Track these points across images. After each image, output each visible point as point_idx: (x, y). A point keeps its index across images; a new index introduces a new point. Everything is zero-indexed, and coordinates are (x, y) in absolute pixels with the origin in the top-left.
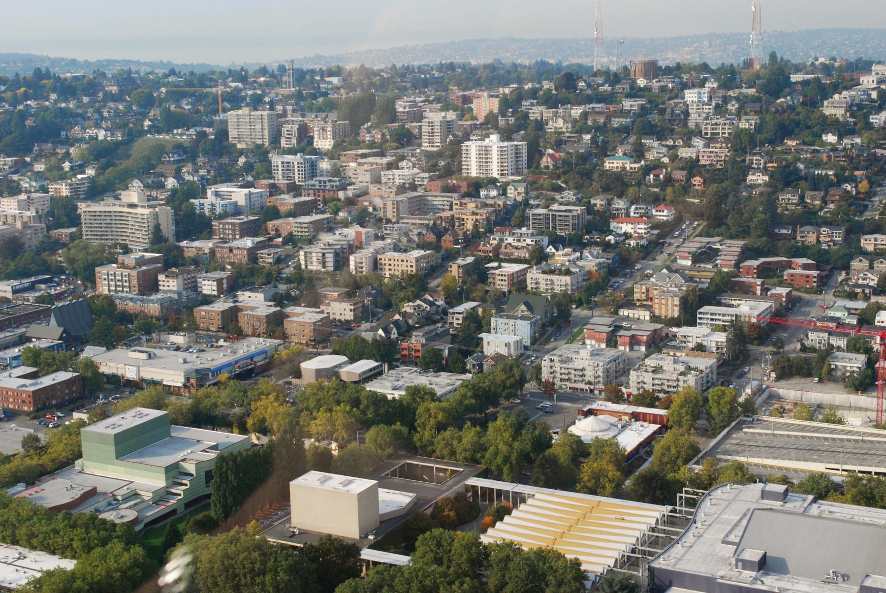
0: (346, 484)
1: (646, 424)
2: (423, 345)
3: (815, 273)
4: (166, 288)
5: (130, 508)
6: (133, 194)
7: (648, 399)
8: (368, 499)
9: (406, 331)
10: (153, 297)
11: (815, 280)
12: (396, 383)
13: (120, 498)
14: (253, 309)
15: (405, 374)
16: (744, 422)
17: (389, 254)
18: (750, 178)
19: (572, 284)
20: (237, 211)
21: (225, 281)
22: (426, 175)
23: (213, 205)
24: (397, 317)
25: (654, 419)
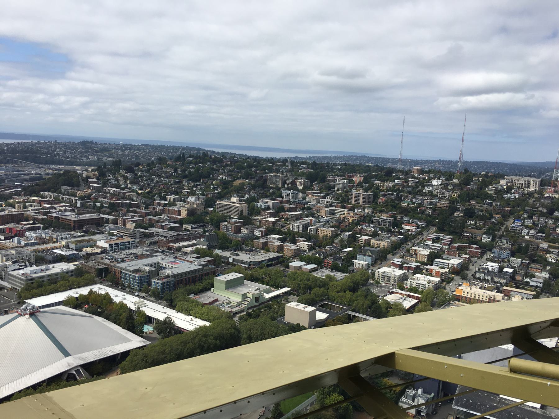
0: (304, 308)
1: (413, 299)
2: (332, 262)
3: (480, 251)
4: (244, 232)
5: (229, 307)
6: (234, 199)
7: (414, 290)
8: (313, 314)
9: (326, 256)
10: (239, 235)
11: (479, 254)
12: (322, 274)
13: (225, 303)
14: (273, 242)
15: (325, 271)
16: (451, 303)
17: (322, 228)
18: (456, 213)
19: (387, 246)
20: (268, 208)
21: (264, 232)
22: (336, 202)
23: (261, 205)
24: (324, 251)
25: (417, 298)
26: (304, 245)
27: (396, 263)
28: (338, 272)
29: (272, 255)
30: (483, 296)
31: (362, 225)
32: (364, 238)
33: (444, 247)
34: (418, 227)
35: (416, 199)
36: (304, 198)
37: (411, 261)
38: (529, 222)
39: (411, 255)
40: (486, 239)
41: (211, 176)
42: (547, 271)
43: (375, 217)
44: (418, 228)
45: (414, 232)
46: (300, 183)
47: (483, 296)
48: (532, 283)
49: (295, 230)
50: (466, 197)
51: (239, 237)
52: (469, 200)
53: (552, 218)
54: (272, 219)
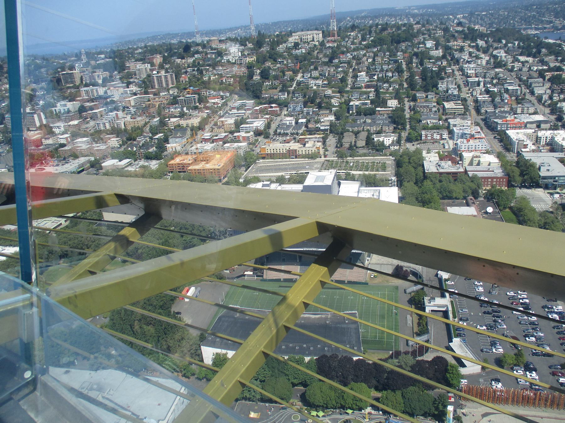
4: (46, 143)
10: (41, 147)
15: (140, 163)
22: (140, 89)
26: (114, 142)
27: (206, 138)
28: (152, 161)
29: (82, 160)
30: (283, 149)
31: (169, 108)
32: (173, 120)
33: (248, 112)
34: (222, 97)
35: (217, 70)
36: (106, 92)
37: (220, 133)
38: (315, 74)
39: (219, 127)
40: (284, 96)
42: (332, 115)
43: (180, 97)
44: (222, 100)
45: (219, 104)
46: (98, 76)
47: (283, 149)
48: (322, 128)
49: (102, 129)
50: (261, 60)
51: (41, 149)
52: (264, 63)
53: (333, 66)
54: (76, 122)
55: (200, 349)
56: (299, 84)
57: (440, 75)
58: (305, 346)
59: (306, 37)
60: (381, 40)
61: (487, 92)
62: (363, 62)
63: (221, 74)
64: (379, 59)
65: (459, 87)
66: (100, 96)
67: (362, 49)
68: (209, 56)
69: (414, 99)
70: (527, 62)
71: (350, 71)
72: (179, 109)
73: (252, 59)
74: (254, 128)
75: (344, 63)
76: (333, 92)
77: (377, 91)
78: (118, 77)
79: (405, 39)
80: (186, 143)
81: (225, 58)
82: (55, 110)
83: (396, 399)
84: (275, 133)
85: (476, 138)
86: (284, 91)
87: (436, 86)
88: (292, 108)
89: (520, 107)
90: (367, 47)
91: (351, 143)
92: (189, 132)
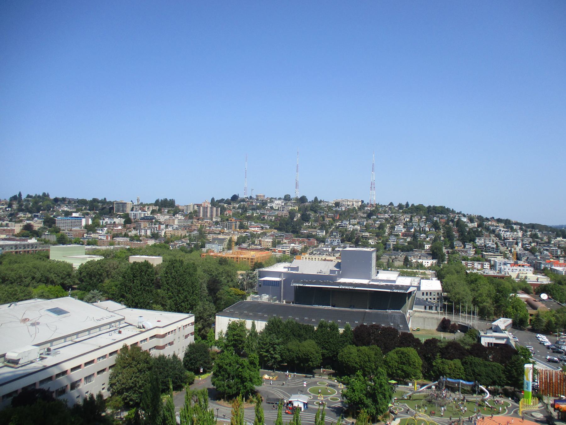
31: (210, 227)
34: (262, 228)
38: (353, 221)
41: (52, 209)
55: (215, 318)
56: (337, 227)
57: (477, 234)
58: (338, 321)
59: (347, 203)
60: (418, 208)
61: (526, 249)
62: (400, 220)
63: (264, 213)
64: (416, 219)
65: (496, 243)
66: (147, 216)
67: (399, 213)
68: (254, 204)
69: (452, 247)
70: (563, 241)
71: (388, 225)
72: (220, 229)
73: (294, 208)
74: (291, 247)
75: (382, 219)
76: (370, 236)
77: (414, 236)
78: (166, 211)
79: (441, 212)
80: (222, 251)
81: (269, 205)
82: (103, 222)
83: (454, 364)
84: (312, 253)
85: (520, 266)
86: (323, 230)
87: (473, 240)
88: (329, 242)
89: (562, 260)
90: (404, 212)
91: (389, 261)
92: (226, 243)
